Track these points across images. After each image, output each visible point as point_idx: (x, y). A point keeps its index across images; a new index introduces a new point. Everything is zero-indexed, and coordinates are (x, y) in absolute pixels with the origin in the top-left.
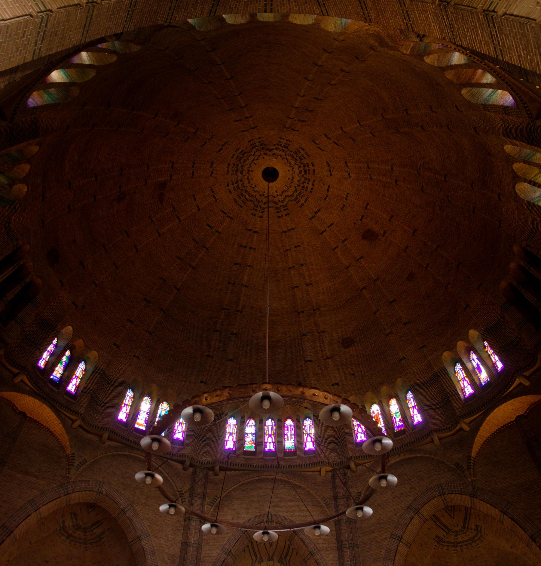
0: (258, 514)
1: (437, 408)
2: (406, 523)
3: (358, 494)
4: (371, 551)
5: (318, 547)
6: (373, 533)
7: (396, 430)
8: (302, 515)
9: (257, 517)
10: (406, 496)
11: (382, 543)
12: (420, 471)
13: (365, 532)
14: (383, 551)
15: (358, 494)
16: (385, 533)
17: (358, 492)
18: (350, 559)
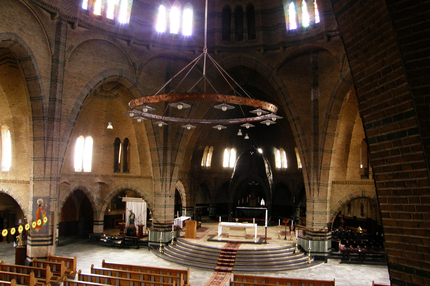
0: (8, 31)
1: (139, 24)
2: (97, 82)
3: (72, 47)
4: (71, 89)
5: (41, 74)
6: (75, 78)
7: (252, 153)
8: (36, 45)
9: (7, 33)
10: (101, 66)
11: (78, 88)
12: (114, 55)
13: (70, 76)
14: (79, 93)
15: (72, 47)
16: (83, 82)
17: (72, 45)
18: (59, 90)
